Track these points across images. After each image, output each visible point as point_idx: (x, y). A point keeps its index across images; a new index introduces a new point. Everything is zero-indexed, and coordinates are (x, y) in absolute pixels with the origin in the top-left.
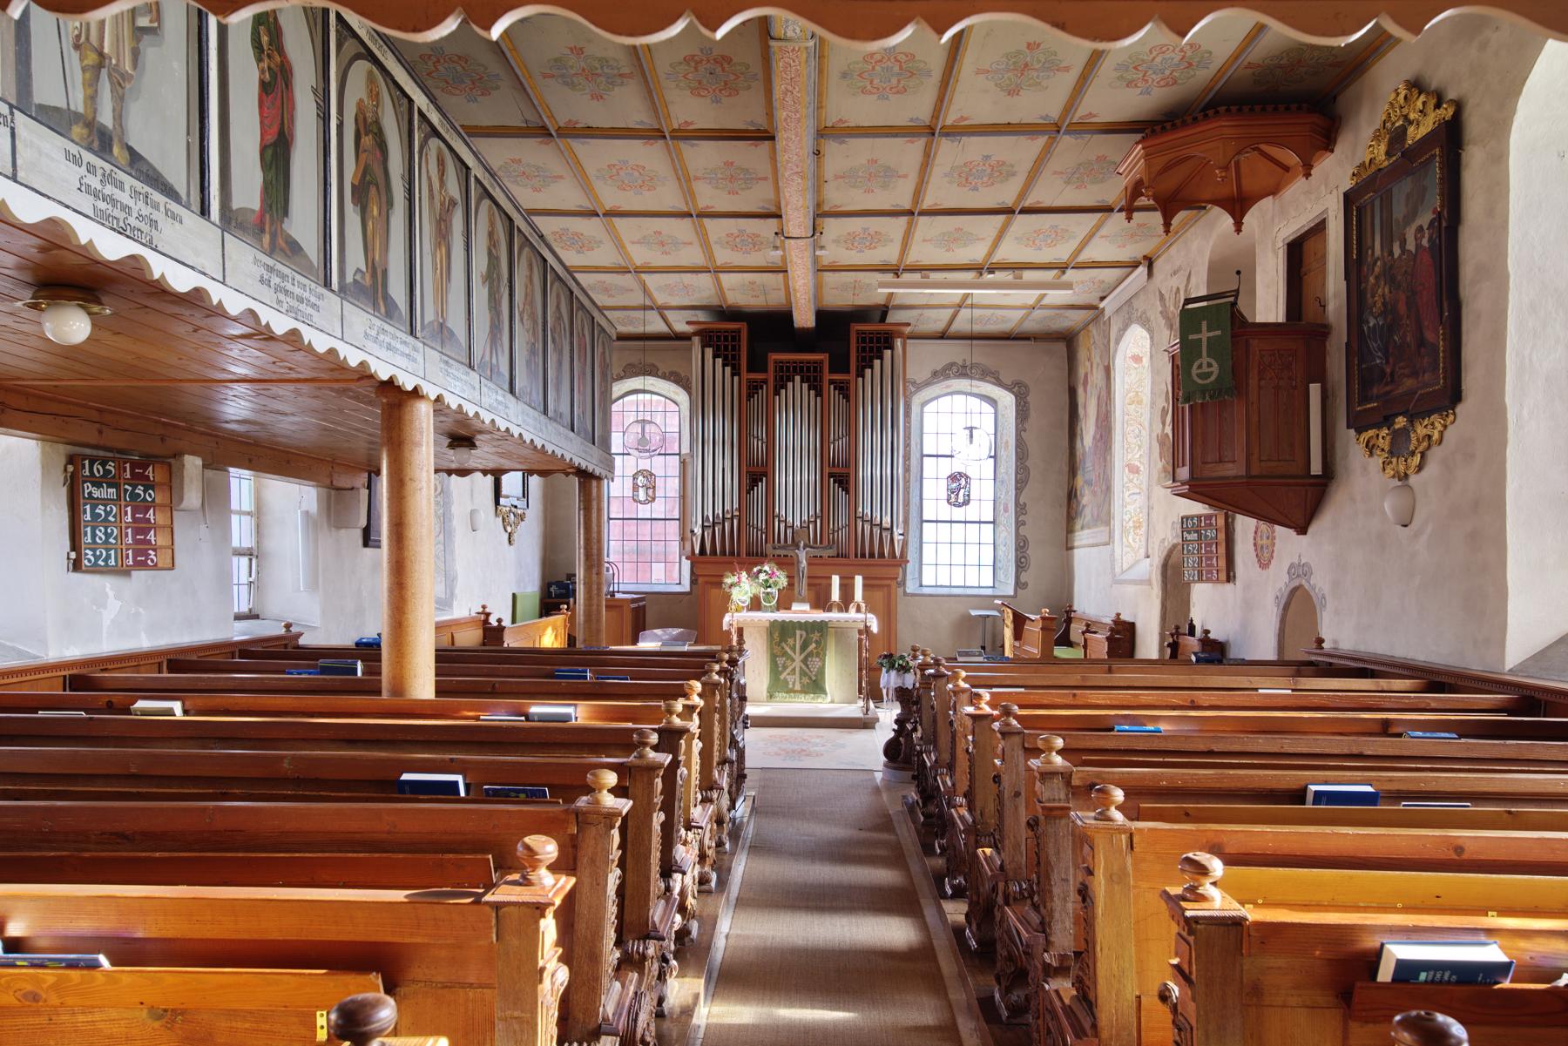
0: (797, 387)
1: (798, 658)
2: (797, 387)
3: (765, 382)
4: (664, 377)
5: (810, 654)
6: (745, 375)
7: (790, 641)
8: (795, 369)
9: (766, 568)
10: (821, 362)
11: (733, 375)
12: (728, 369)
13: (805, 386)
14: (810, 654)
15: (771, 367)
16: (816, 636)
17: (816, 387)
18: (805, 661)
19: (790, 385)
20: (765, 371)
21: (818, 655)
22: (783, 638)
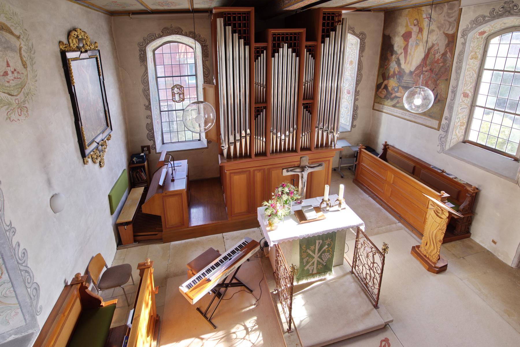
0: (285, 51)
1: (316, 256)
2: (285, 51)
3: (266, 48)
4: (186, 35)
5: (324, 252)
6: (254, 45)
7: (312, 248)
8: (283, 38)
9: (286, 190)
10: (300, 33)
11: (245, 45)
12: (242, 41)
13: (290, 50)
14: (324, 252)
15: (270, 39)
16: (328, 242)
17: (298, 52)
18: (320, 257)
19: (281, 50)
20: (265, 40)
21: (328, 251)
22: (308, 247)
